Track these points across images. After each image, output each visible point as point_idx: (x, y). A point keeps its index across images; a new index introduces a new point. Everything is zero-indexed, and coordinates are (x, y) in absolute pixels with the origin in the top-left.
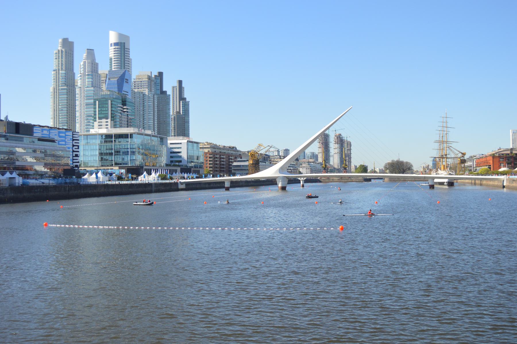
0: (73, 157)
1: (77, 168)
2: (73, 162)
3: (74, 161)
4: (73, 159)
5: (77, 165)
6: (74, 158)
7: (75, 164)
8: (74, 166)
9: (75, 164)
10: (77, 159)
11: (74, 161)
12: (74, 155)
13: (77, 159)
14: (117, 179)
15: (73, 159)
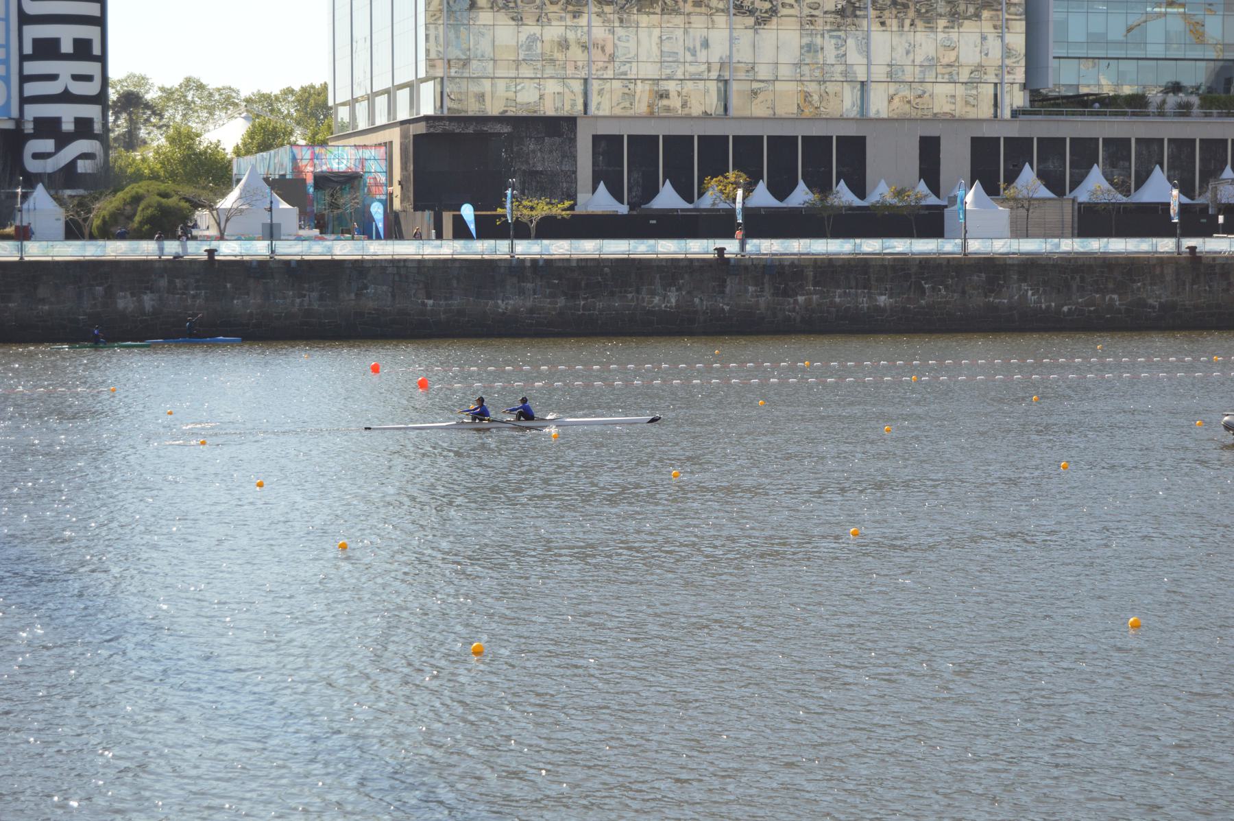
0: (23, 58)
1: (48, 145)
2: (24, 100)
3: (32, 89)
4: (24, 79)
5: (57, 121)
6: (32, 68)
7: (33, 111)
8: (29, 128)
9: (33, 111)
10: (53, 77)
11: (32, 89)
12: (28, 49)
13: (53, 77)
14: (60, 227)
15: (24, 79)
